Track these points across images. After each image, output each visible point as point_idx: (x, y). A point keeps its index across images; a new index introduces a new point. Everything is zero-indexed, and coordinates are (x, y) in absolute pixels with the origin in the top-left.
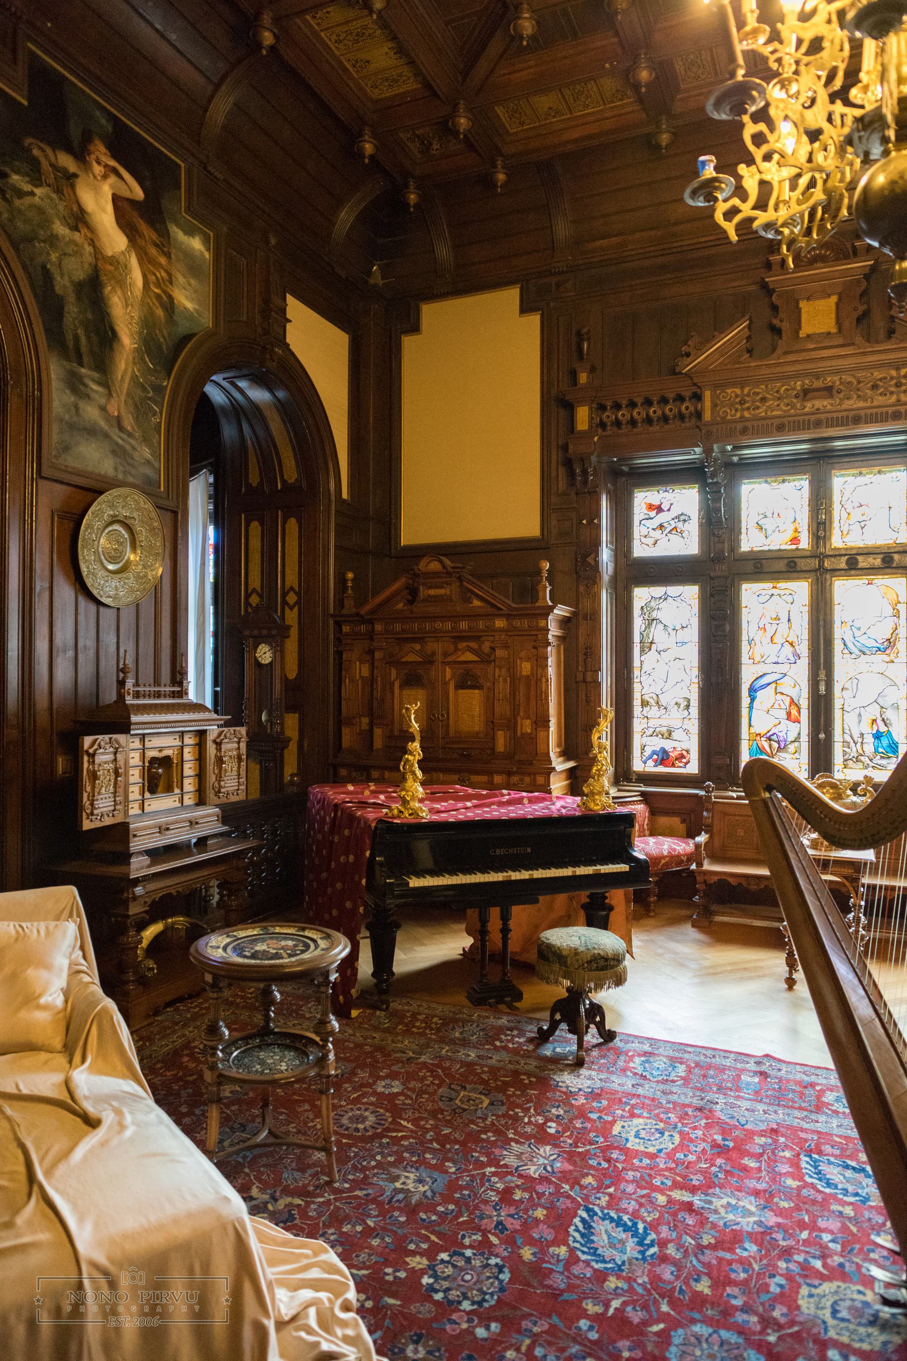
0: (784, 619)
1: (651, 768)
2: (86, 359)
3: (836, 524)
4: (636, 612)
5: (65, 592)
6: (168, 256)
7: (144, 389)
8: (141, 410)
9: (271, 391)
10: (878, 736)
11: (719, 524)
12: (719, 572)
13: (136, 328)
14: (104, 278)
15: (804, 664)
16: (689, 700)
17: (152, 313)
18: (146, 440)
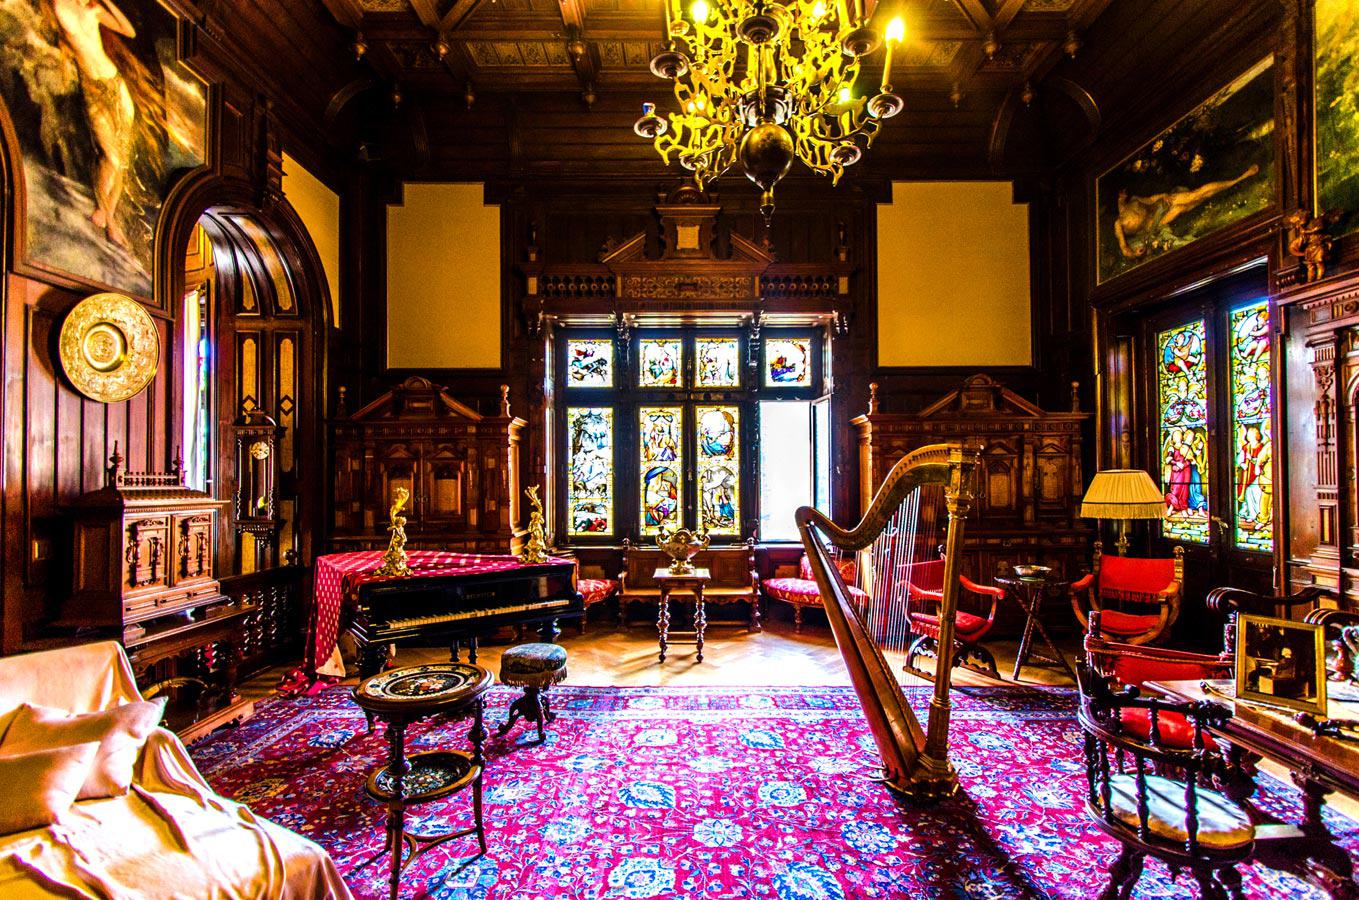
0: (666, 430)
1: (580, 532)
2: (67, 168)
4: (570, 425)
5: (42, 384)
6: (162, 94)
7: (135, 207)
8: (132, 226)
9: (267, 230)
10: (722, 507)
11: (626, 366)
12: (626, 398)
13: (127, 152)
14: (89, 99)
15: (679, 460)
16: (605, 486)
17: (145, 142)
18: (137, 254)
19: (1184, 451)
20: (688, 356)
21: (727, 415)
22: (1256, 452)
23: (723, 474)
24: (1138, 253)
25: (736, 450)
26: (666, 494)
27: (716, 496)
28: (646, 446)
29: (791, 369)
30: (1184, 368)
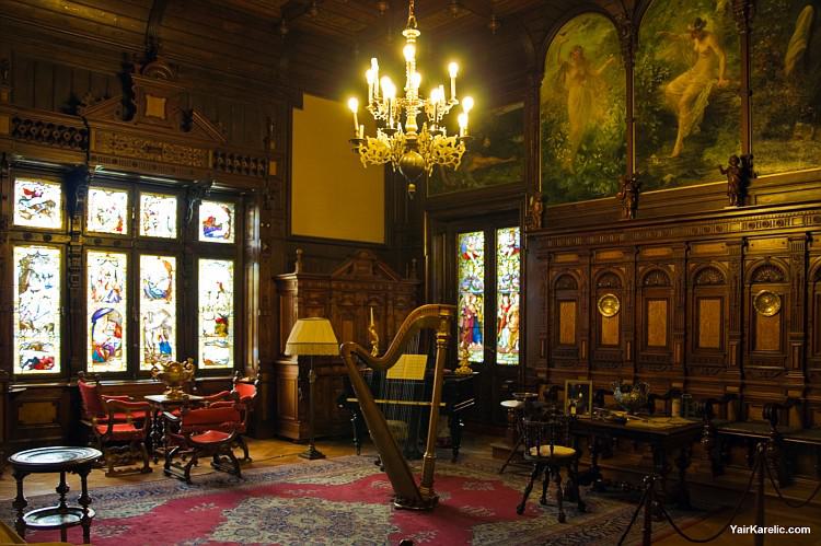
1: (27, 371)
3: (142, 223)
10: (162, 344)
12: (75, 247)
16: (53, 325)
19: (471, 308)
20: (134, 206)
21: (166, 263)
22: (507, 309)
23: (163, 316)
24: (453, 184)
25: (173, 294)
26: (112, 333)
27: (156, 335)
28: (93, 287)
29: (219, 228)
30: (472, 257)
